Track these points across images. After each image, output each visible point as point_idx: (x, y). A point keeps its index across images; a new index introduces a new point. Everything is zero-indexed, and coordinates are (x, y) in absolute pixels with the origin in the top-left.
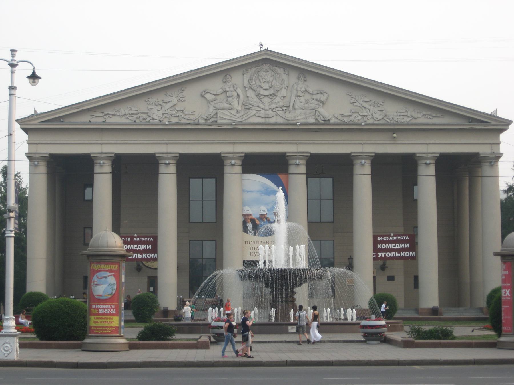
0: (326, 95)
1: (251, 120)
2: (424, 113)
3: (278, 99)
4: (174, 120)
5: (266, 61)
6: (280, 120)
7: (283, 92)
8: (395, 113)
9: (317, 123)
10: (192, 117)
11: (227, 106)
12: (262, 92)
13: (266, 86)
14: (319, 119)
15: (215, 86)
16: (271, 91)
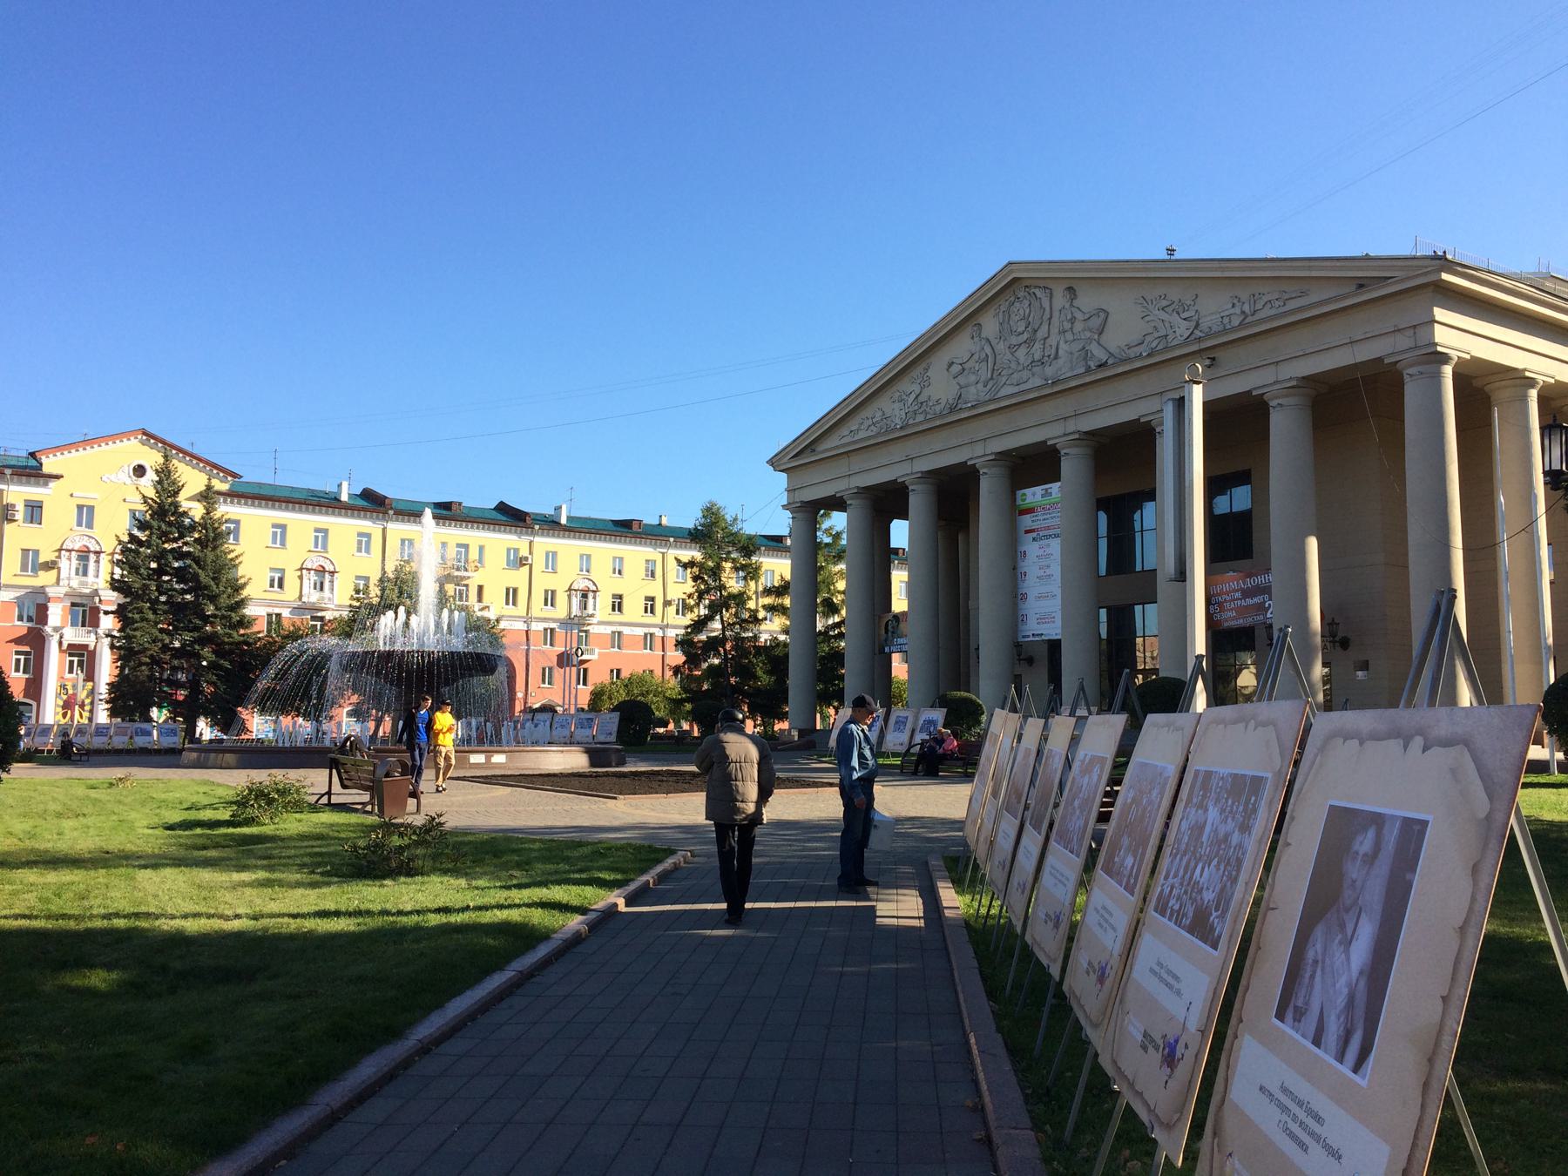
0: (1102, 315)
1: (1003, 392)
2: (1265, 299)
3: (1038, 346)
4: (920, 418)
5: (1015, 280)
6: (1038, 382)
7: (1045, 327)
8: (1214, 310)
9: (1088, 370)
10: (938, 408)
11: (973, 378)
12: (1014, 340)
13: (1021, 329)
14: (1092, 365)
15: (962, 347)
16: (1026, 336)
